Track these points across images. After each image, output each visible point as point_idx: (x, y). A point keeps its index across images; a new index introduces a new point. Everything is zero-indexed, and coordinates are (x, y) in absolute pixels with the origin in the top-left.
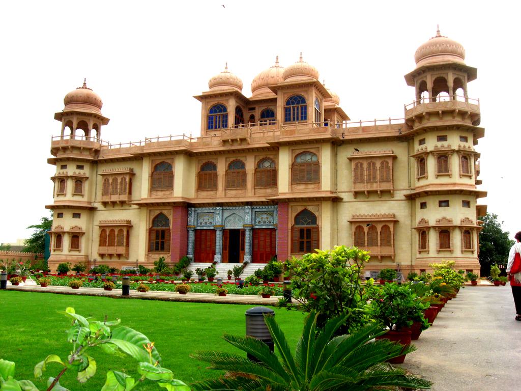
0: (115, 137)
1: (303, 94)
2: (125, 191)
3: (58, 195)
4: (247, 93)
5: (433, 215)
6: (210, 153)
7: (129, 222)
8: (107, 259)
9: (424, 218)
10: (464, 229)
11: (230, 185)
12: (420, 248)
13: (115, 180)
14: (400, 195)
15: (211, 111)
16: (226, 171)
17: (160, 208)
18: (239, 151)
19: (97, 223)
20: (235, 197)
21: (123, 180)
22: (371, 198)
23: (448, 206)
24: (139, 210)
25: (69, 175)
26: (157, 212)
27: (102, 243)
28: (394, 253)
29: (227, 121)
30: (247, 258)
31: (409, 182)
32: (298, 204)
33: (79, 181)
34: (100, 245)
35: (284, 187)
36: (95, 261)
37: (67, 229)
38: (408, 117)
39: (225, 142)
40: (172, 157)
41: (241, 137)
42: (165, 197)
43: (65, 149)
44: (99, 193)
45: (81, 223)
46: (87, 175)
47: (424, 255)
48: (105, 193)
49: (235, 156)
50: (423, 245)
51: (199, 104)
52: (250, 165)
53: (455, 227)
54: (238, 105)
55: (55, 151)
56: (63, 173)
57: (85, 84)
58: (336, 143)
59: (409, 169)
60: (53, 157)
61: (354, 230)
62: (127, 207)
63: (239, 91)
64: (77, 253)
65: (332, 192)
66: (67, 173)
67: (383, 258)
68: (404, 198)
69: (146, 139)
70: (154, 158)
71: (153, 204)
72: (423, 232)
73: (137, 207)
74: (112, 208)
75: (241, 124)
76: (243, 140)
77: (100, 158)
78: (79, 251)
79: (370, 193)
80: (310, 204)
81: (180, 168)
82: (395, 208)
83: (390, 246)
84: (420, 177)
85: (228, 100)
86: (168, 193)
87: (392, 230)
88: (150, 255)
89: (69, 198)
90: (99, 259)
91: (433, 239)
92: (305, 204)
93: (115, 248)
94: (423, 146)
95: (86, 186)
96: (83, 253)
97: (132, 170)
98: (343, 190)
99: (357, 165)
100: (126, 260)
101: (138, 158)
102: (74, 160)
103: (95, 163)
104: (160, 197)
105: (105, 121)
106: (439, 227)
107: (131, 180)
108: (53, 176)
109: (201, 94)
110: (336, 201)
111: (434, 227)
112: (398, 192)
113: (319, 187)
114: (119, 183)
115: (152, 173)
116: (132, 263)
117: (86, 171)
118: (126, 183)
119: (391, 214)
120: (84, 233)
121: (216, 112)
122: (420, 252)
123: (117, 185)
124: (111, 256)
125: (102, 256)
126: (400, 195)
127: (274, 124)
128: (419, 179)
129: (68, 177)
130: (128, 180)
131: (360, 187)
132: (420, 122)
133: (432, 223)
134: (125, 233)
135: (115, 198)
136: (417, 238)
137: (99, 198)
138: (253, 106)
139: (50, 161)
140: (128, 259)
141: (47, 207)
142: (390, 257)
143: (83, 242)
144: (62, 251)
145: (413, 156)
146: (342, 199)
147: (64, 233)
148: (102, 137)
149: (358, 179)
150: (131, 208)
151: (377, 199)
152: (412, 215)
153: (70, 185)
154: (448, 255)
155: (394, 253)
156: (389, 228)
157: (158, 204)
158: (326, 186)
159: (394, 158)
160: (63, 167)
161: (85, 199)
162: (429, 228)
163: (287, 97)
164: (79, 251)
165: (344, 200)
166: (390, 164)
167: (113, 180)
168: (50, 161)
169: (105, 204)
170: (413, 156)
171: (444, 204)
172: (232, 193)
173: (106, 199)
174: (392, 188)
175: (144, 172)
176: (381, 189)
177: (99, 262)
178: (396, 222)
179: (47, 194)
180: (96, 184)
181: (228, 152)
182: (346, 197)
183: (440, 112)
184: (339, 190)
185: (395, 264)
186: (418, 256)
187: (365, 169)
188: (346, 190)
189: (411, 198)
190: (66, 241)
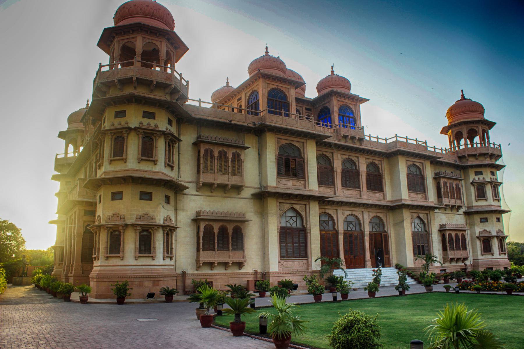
1: (351, 106)
9: (486, 229)
14: (461, 211)
17: (293, 202)
23: (487, 221)
24: (252, 200)
26: (287, 206)
30: (369, 263)
40: (303, 141)
47: (490, 257)
50: (487, 248)
56: (149, 124)
62: (235, 196)
66: (156, 126)
68: (462, 213)
74: (210, 194)
78: (171, 258)
80: (423, 212)
88: (282, 262)
94: (481, 177)
96: (172, 263)
104: (290, 185)
113: (426, 198)
114: (230, 159)
124: (211, 265)
132: (491, 159)
135: (222, 179)
136: (479, 244)
144: (153, 258)
147: (126, 226)
150: (239, 196)
151: (450, 212)
167: (220, 152)
177: (193, 275)
180: (179, 155)
185: (463, 264)
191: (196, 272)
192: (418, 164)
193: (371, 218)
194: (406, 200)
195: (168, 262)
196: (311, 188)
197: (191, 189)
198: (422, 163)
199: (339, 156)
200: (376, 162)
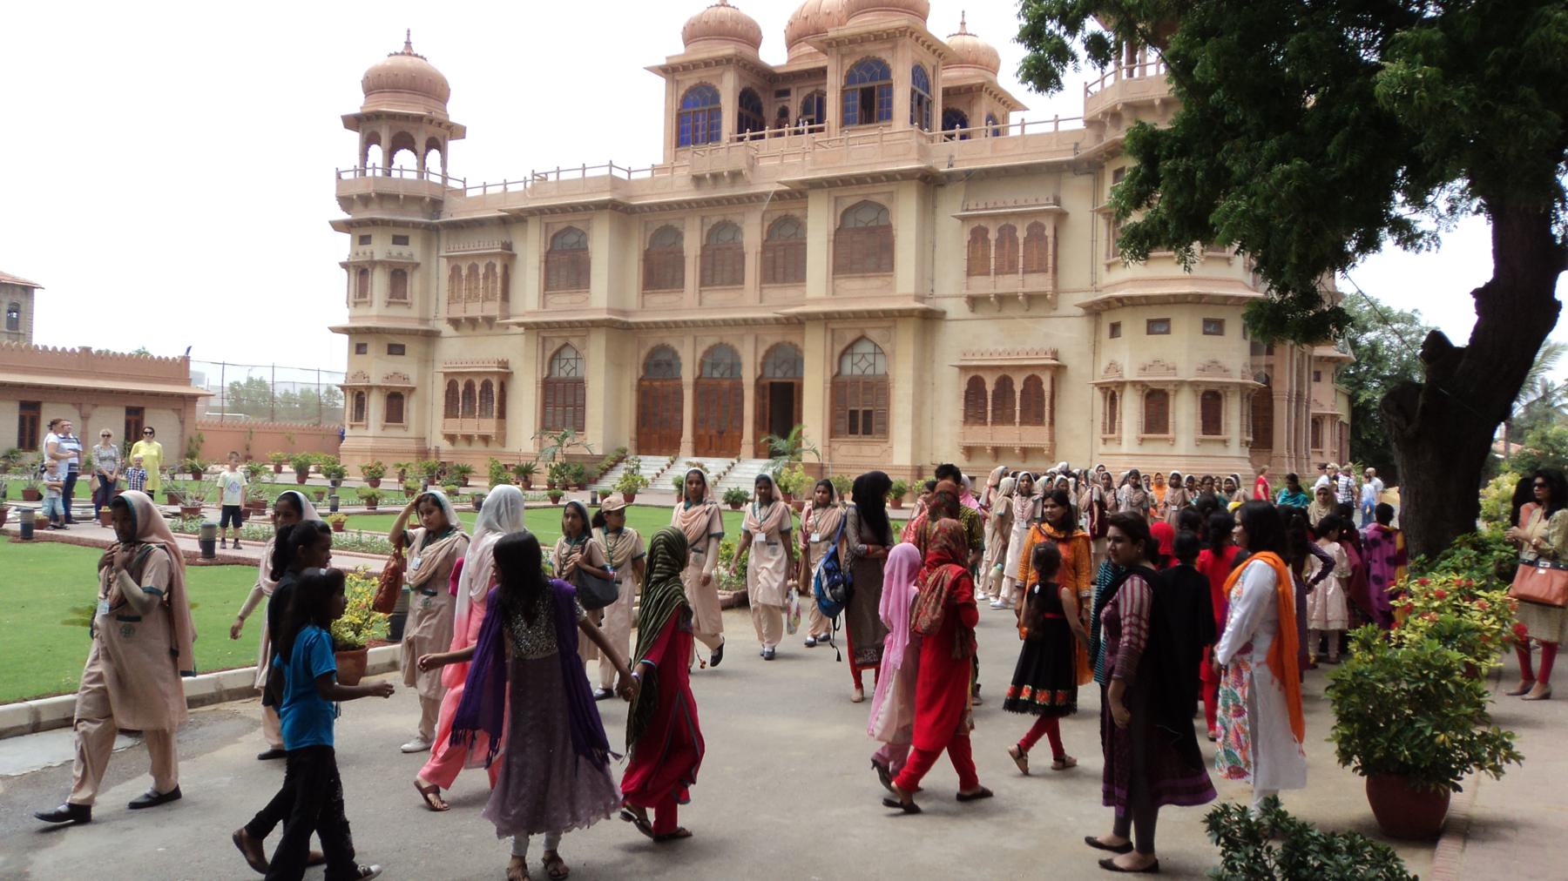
0: (486, 164)
2: (494, 294)
3: (356, 304)
4: (774, 54)
5: (1131, 356)
6: (669, 206)
7: (504, 364)
8: (462, 446)
10: (1202, 389)
11: (708, 279)
12: (1104, 430)
13: (473, 269)
14: (1071, 303)
15: (685, 101)
16: (703, 248)
18: (729, 201)
19: (440, 367)
20: (723, 308)
21: (490, 267)
22: (1007, 312)
25: (377, 257)
27: (450, 411)
28: (1052, 439)
29: (719, 126)
31: (1093, 273)
32: (847, 325)
33: (399, 275)
34: (446, 416)
35: (817, 288)
36: (437, 451)
37: (376, 380)
38: (1091, 114)
39: (698, 180)
41: (732, 168)
42: (573, 307)
43: (365, 200)
44: (444, 297)
45: (406, 368)
46: (417, 259)
47: (1112, 448)
48: (452, 299)
49: (719, 210)
51: (660, 82)
52: (752, 236)
53: (1181, 384)
54: (747, 84)
55: (345, 202)
57: (408, 43)
58: (930, 183)
59: (1094, 241)
60: (345, 216)
61: (964, 387)
63: (747, 50)
64: (399, 433)
65: (920, 298)
67: (1026, 452)
68: (1081, 311)
69: (534, 174)
70: (547, 219)
71: (549, 326)
72: (1111, 394)
73: (521, 330)
75: (748, 134)
76: (736, 175)
77: (445, 218)
78: (406, 428)
79: (1003, 300)
81: (601, 245)
82: (1061, 335)
83: (1040, 422)
84: (1112, 260)
85: (721, 75)
86: (578, 298)
87: (1047, 387)
89: (377, 313)
90: (445, 445)
91: (1131, 410)
92: (861, 324)
93: (476, 421)
95: (415, 283)
96: (412, 432)
97: (508, 246)
98: (946, 292)
99: (974, 232)
100: (499, 449)
101: (512, 221)
102: (384, 223)
103: (432, 231)
104: (565, 308)
105: (458, 132)
106: (1142, 384)
107: (506, 269)
108: (345, 259)
109: (663, 62)
110: (928, 319)
111: (1134, 383)
112: (1067, 296)
115: (548, 254)
116: (512, 454)
117: (414, 250)
118: (494, 274)
119: (1046, 348)
120: (412, 390)
121: (696, 105)
122: (1105, 440)
123: (477, 279)
125: (451, 438)
126: (1071, 303)
127: (821, 130)
128: (1109, 266)
129: (374, 264)
130: (499, 270)
131: (984, 286)
133: (1129, 374)
134: (496, 389)
135: (475, 310)
137: (443, 313)
138: (786, 87)
139: (338, 226)
140: (503, 444)
141: (335, 330)
142: (1041, 450)
143: (411, 407)
145: (1099, 211)
146: (944, 313)
148: (450, 171)
149: (975, 267)
151: (1023, 313)
152: (1095, 348)
153: (379, 283)
154: (1162, 448)
155: (1052, 439)
156: (1039, 383)
157: (560, 326)
158: (902, 287)
159: (1061, 217)
160: (364, 240)
161: (415, 312)
162: (1121, 385)
163: (848, 63)
164: (406, 428)
165: (950, 315)
166: (1049, 232)
168: (338, 226)
169: (455, 323)
170: (1099, 211)
171: (1157, 327)
172: (715, 297)
173: (458, 312)
174: (1050, 288)
175: (530, 252)
176: (1027, 290)
177: (447, 453)
178: (1058, 370)
179: (333, 300)
181: (709, 203)
182: (954, 307)
183: (1157, 102)
184: (937, 293)
186: (1102, 449)
187: (993, 243)
188: (953, 292)
189: (1095, 311)
190: (376, 407)
191: (451, 448)
192: (876, 199)
193: (766, 347)
194: (817, 301)
195: (395, 431)
196: (594, 305)
197: (446, 329)
198: (891, 193)
199: (697, 222)
200: (797, 213)
